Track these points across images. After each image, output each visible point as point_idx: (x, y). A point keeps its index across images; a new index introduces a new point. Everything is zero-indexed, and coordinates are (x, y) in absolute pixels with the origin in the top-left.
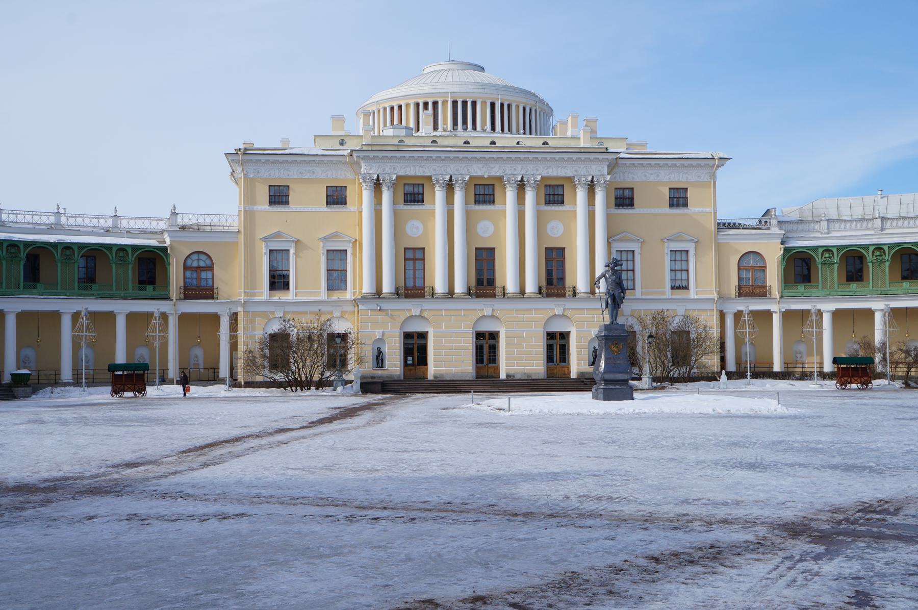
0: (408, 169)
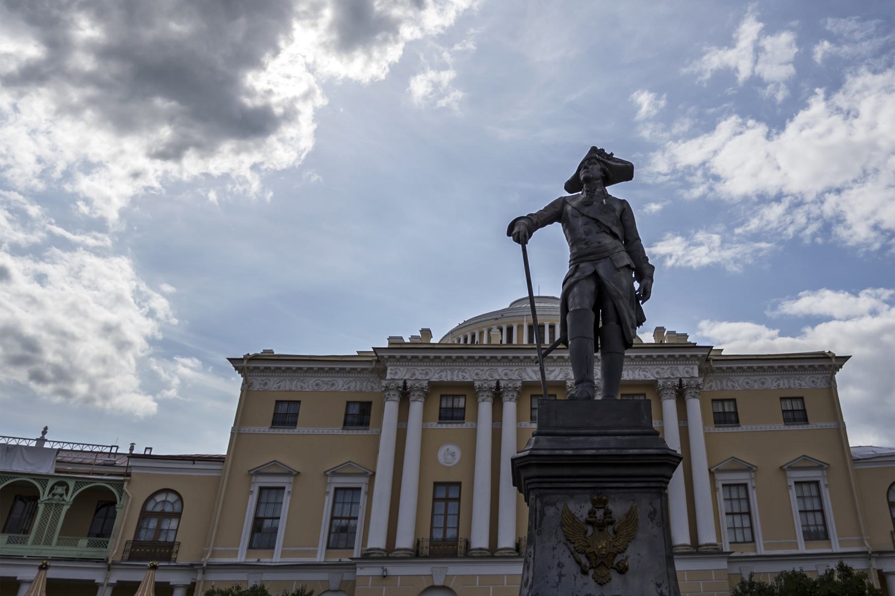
0: (444, 374)
